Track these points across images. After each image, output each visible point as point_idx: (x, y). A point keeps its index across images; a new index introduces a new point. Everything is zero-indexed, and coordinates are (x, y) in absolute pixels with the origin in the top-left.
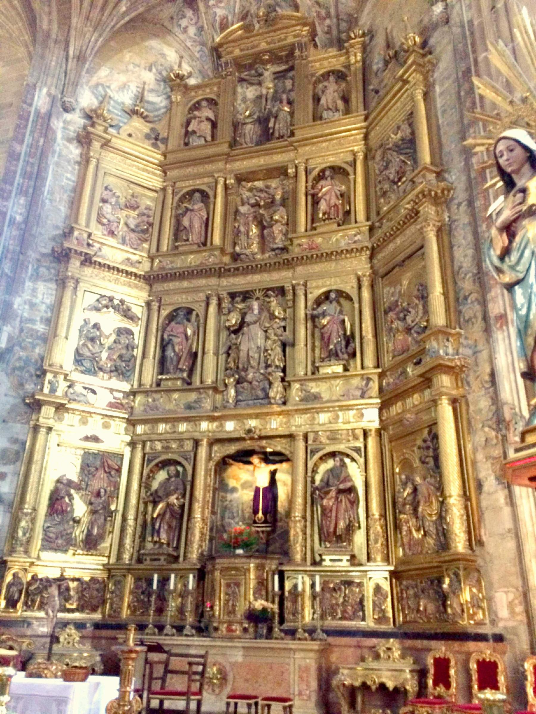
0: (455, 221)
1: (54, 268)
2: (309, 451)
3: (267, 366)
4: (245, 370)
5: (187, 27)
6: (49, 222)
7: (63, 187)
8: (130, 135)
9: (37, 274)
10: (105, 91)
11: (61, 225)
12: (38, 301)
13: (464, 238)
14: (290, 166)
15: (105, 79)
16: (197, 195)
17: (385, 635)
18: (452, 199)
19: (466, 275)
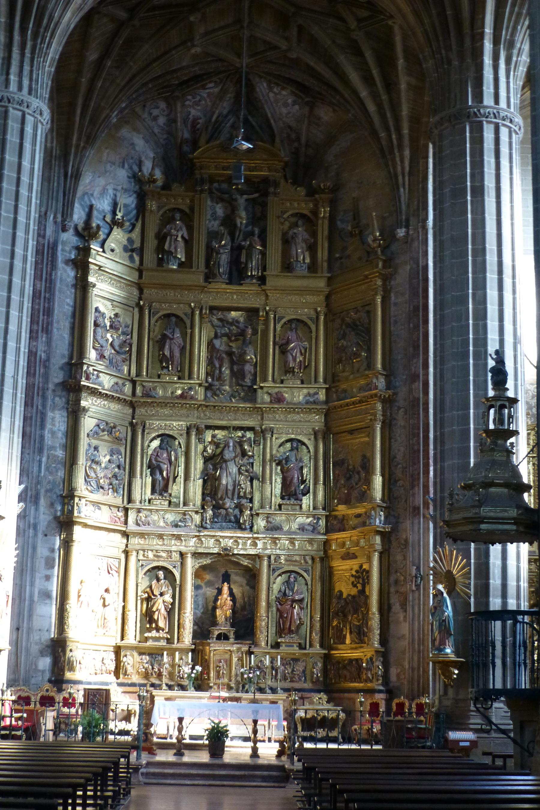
1: (64, 396)
3: (239, 497)
4: (222, 498)
5: (158, 116)
6: (58, 351)
7: (64, 314)
8: (112, 250)
9: (54, 403)
10: (90, 201)
11: (66, 353)
12: (56, 429)
14: (261, 310)
15: (88, 187)
16: (174, 319)
17: (319, 691)
19: (398, 464)
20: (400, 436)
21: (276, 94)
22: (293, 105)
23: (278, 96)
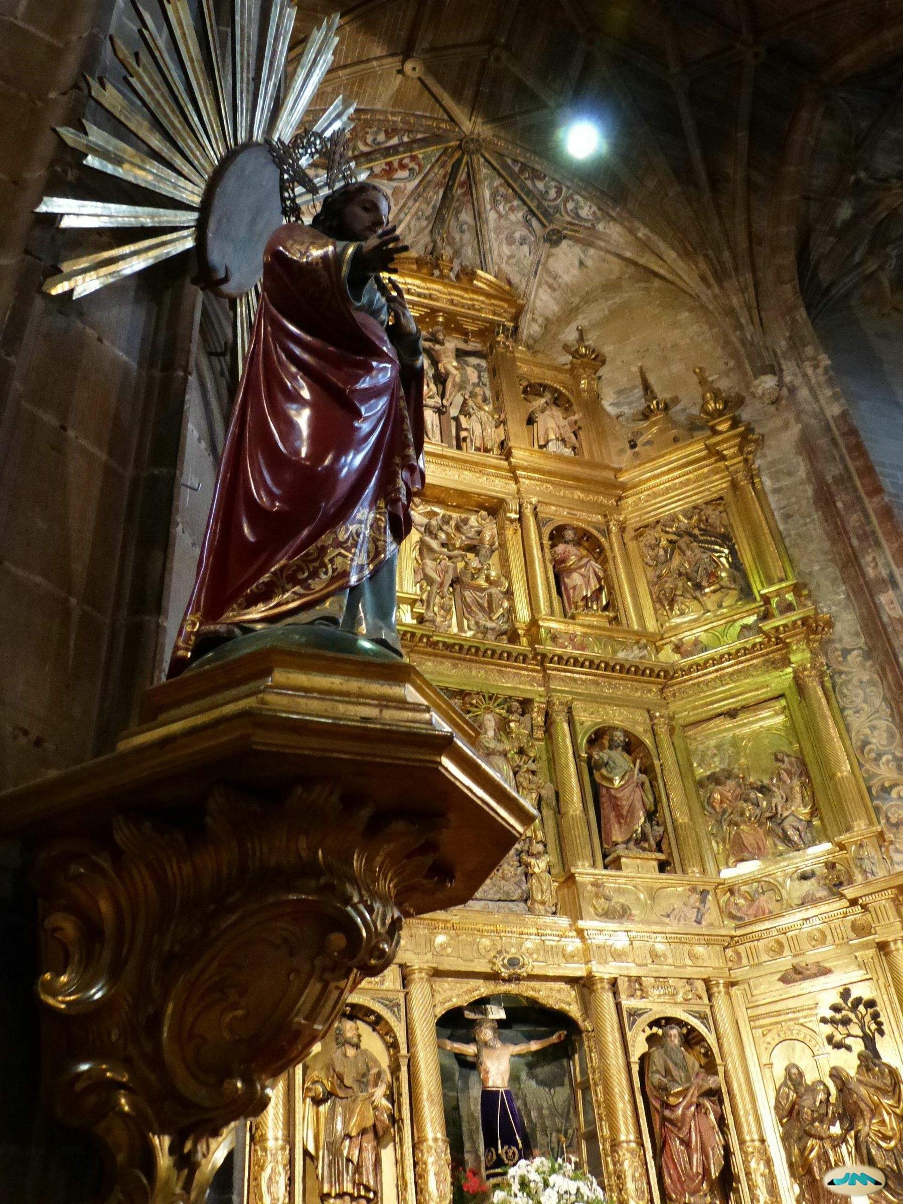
0: (840, 673)
2: (625, 1015)
13: (865, 701)
18: (830, 641)
19: (879, 756)
20: (865, 701)
21: (500, 216)
22: (521, 244)
23: (503, 221)
